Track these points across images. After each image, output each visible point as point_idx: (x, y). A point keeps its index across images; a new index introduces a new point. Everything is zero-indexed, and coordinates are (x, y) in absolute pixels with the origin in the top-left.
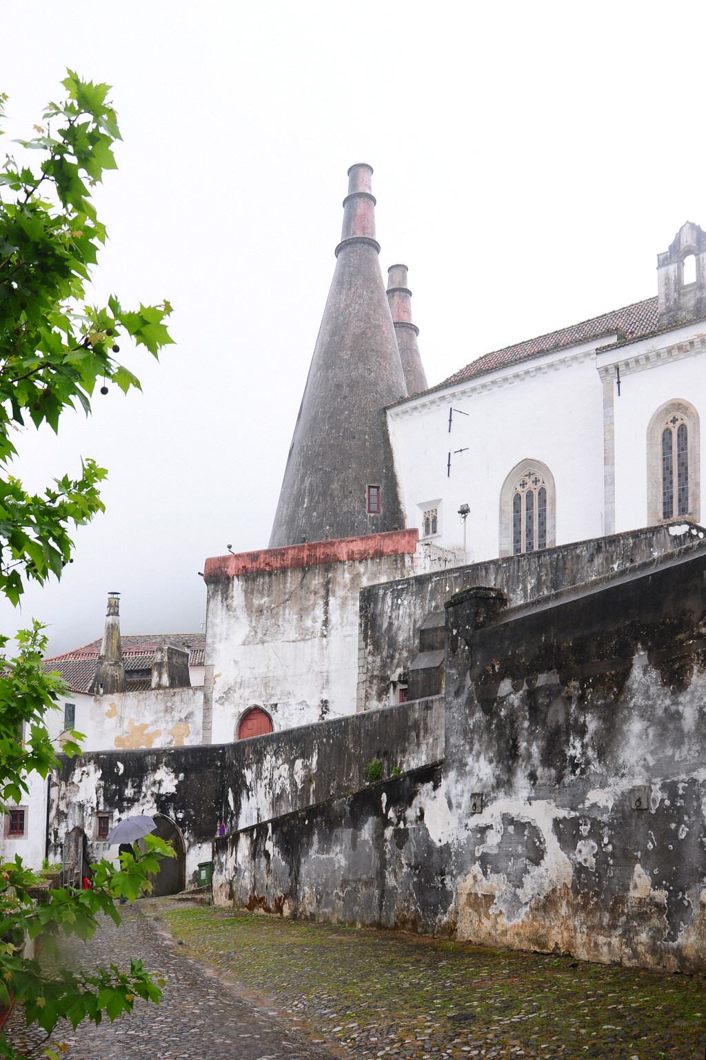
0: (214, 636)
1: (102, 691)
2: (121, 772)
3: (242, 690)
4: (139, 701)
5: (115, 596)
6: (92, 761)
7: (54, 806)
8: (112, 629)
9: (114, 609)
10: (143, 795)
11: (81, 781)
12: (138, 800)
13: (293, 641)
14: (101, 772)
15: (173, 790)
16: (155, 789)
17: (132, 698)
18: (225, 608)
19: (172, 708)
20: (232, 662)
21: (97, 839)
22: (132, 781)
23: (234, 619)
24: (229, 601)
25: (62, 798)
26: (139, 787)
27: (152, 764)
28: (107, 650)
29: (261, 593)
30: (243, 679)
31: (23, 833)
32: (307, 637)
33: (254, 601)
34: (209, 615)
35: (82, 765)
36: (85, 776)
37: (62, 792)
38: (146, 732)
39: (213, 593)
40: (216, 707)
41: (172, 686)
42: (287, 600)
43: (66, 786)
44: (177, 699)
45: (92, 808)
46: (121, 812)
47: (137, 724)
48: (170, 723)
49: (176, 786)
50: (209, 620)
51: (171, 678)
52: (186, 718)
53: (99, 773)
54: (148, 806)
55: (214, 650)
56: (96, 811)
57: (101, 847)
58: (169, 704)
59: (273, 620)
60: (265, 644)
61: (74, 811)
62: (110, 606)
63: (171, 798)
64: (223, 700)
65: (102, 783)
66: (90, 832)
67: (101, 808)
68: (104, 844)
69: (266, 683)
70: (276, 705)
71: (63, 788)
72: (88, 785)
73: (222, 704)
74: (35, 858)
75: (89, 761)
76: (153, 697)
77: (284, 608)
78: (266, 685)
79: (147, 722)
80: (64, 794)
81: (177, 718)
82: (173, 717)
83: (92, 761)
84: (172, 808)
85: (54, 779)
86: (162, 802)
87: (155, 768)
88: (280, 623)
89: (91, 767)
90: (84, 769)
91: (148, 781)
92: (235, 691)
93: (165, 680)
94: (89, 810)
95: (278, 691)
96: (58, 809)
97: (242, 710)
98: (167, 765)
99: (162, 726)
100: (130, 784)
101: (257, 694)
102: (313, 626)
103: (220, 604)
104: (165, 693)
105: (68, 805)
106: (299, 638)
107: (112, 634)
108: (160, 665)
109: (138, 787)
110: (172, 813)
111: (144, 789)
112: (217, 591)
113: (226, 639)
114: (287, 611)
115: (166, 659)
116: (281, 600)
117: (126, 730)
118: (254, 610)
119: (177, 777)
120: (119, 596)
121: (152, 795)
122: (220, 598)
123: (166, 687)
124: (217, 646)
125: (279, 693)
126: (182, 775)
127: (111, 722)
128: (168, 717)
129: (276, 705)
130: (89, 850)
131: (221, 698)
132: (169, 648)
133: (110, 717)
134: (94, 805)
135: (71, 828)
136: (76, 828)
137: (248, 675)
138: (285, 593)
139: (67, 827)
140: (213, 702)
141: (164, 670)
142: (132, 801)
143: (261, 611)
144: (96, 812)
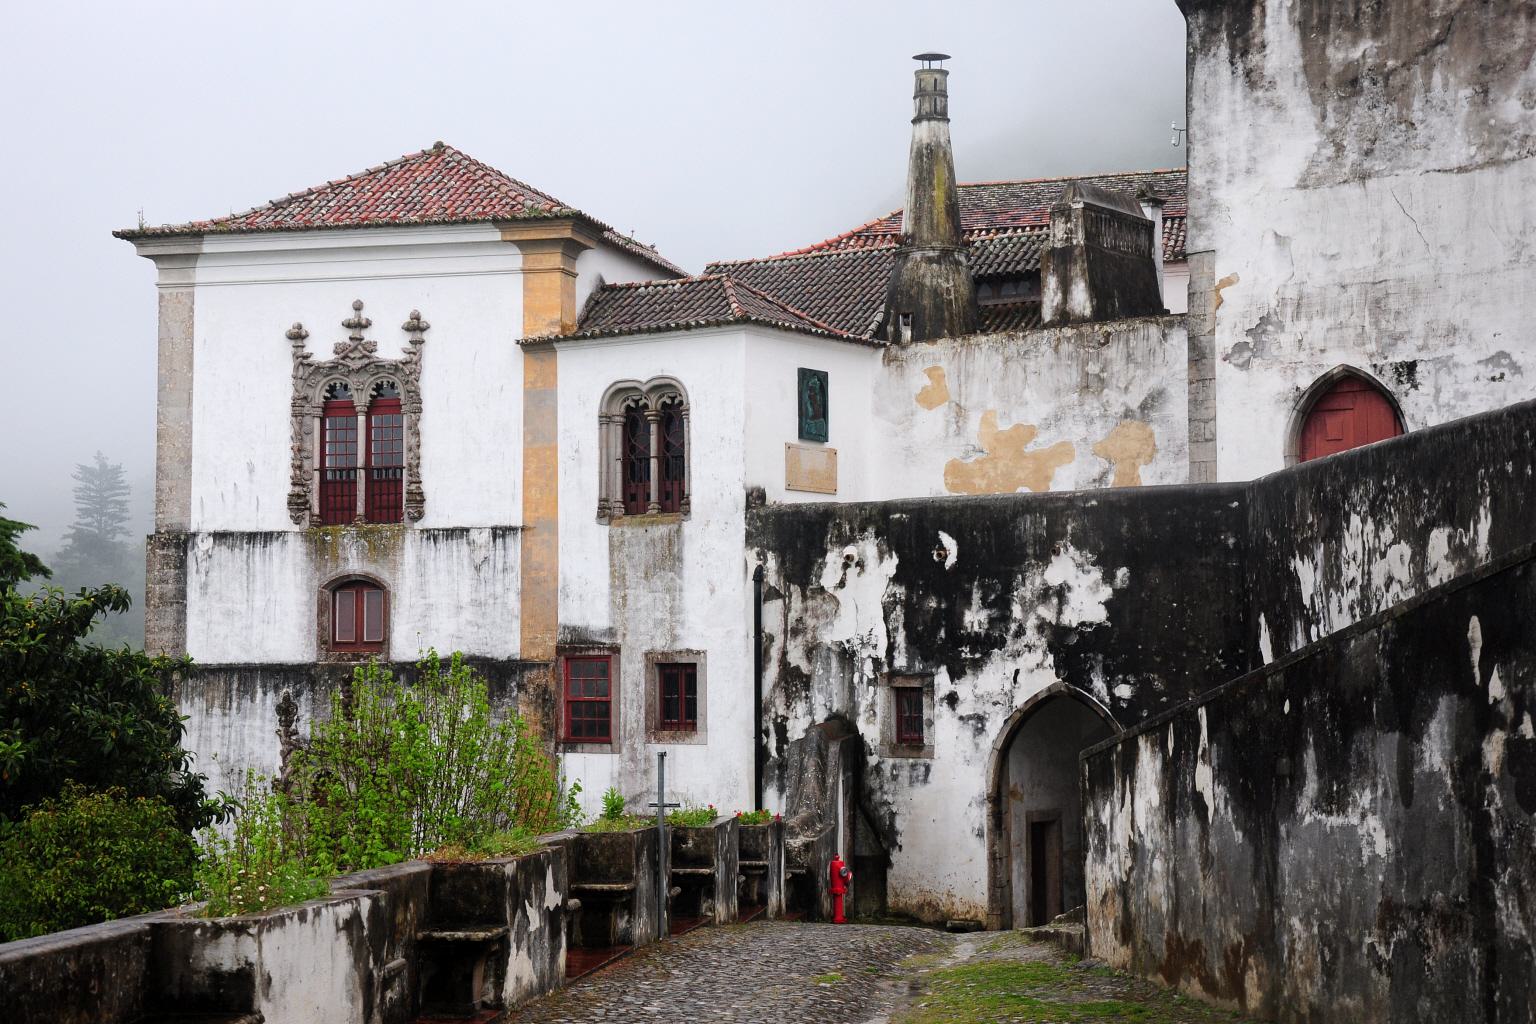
0: (1213, 165)
1: (907, 334)
2: (951, 560)
3: (1303, 324)
4: (1006, 361)
5: (936, 65)
6: (871, 530)
7: (775, 653)
8: (930, 162)
9: (932, 101)
10: (1013, 627)
11: (842, 584)
12: (1001, 643)
13: (1461, 170)
14: (895, 560)
15: (1099, 615)
16: (1047, 613)
17: (987, 354)
18: (1241, 81)
19: (1102, 380)
20: (1270, 240)
21: (894, 751)
22: (981, 586)
23: (1270, 112)
24: (1254, 59)
25: (795, 632)
27: (1038, 539)
28: (917, 220)
29: (1354, 28)
30: (1307, 289)
31: (693, 727)
32: (1508, 154)
33: (1330, 51)
34: (1196, 103)
35: (844, 541)
36: (853, 571)
37: (793, 616)
38: (1030, 448)
39: (1203, 40)
40: (1225, 373)
41: (1101, 314)
42: (1439, 42)
43: (804, 598)
44: (1114, 352)
45: (876, 662)
46: (956, 674)
47: (1004, 426)
48: (1099, 424)
49: (1108, 604)
50: (1195, 117)
51: (1095, 290)
52: (1143, 407)
53: (891, 564)
54: (1029, 660)
55: (1213, 205)
56: (886, 669)
57: (905, 773)
58: (1093, 368)
59: (1393, 109)
60: (1371, 183)
61: (827, 670)
62: (920, 93)
64: (1247, 352)
65: (900, 591)
66: (871, 731)
67: (900, 661)
68: (913, 767)
69: (1377, 301)
70: (1411, 367)
71: (796, 603)
72: (862, 597)
73: (1245, 366)
75: (863, 530)
76: (1044, 348)
77: (1429, 69)
78: (1377, 306)
79: (1034, 420)
80: (800, 620)
81: (1117, 409)
82: (1105, 406)
83: (871, 530)
84: (1099, 668)
85: (772, 579)
86: (1071, 649)
87: (1046, 553)
88: (1416, 115)
89: (868, 547)
90: (850, 550)
91: (1027, 590)
92: (1281, 327)
93: (1081, 300)
94: (868, 667)
95: (1417, 323)
97: (1306, 382)
98: (1079, 544)
99: (1075, 431)
100: (976, 596)
101: (1350, 333)
102: (1525, 120)
103: (1225, 70)
104: (1081, 336)
105: (811, 651)
106: (1479, 159)
107: (931, 172)
108: (1063, 257)
109: (1000, 606)
110: (1099, 684)
111: (1017, 611)
112: (1216, 31)
113: (1248, 171)
114: (1437, 78)
115: (1079, 239)
116: (1418, 42)
117: (975, 441)
118: (1330, 79)
119: (1108, 578)
120: (945, 65)
122: (1224, 51)
123: (1082, 320)
124: (1222, 194)
125: (1419, 329)
126: (1122, 573)
127: (932, 422)
128: (1092, 406)
129: (1411, 367)
130: (873, 782)
131: (1240, 347)
132: (1087, 207)
133: (930, 406)
134: (881, 653)
135: (820, 716)
136: (833, 717)
137: (1318, 276)
138: (1429, 22)
139: (810, 712)
140: (1218, 361)
141: (1077, 270)
142: (987, 644)
143: (1354, 82)
144: (886, 674)
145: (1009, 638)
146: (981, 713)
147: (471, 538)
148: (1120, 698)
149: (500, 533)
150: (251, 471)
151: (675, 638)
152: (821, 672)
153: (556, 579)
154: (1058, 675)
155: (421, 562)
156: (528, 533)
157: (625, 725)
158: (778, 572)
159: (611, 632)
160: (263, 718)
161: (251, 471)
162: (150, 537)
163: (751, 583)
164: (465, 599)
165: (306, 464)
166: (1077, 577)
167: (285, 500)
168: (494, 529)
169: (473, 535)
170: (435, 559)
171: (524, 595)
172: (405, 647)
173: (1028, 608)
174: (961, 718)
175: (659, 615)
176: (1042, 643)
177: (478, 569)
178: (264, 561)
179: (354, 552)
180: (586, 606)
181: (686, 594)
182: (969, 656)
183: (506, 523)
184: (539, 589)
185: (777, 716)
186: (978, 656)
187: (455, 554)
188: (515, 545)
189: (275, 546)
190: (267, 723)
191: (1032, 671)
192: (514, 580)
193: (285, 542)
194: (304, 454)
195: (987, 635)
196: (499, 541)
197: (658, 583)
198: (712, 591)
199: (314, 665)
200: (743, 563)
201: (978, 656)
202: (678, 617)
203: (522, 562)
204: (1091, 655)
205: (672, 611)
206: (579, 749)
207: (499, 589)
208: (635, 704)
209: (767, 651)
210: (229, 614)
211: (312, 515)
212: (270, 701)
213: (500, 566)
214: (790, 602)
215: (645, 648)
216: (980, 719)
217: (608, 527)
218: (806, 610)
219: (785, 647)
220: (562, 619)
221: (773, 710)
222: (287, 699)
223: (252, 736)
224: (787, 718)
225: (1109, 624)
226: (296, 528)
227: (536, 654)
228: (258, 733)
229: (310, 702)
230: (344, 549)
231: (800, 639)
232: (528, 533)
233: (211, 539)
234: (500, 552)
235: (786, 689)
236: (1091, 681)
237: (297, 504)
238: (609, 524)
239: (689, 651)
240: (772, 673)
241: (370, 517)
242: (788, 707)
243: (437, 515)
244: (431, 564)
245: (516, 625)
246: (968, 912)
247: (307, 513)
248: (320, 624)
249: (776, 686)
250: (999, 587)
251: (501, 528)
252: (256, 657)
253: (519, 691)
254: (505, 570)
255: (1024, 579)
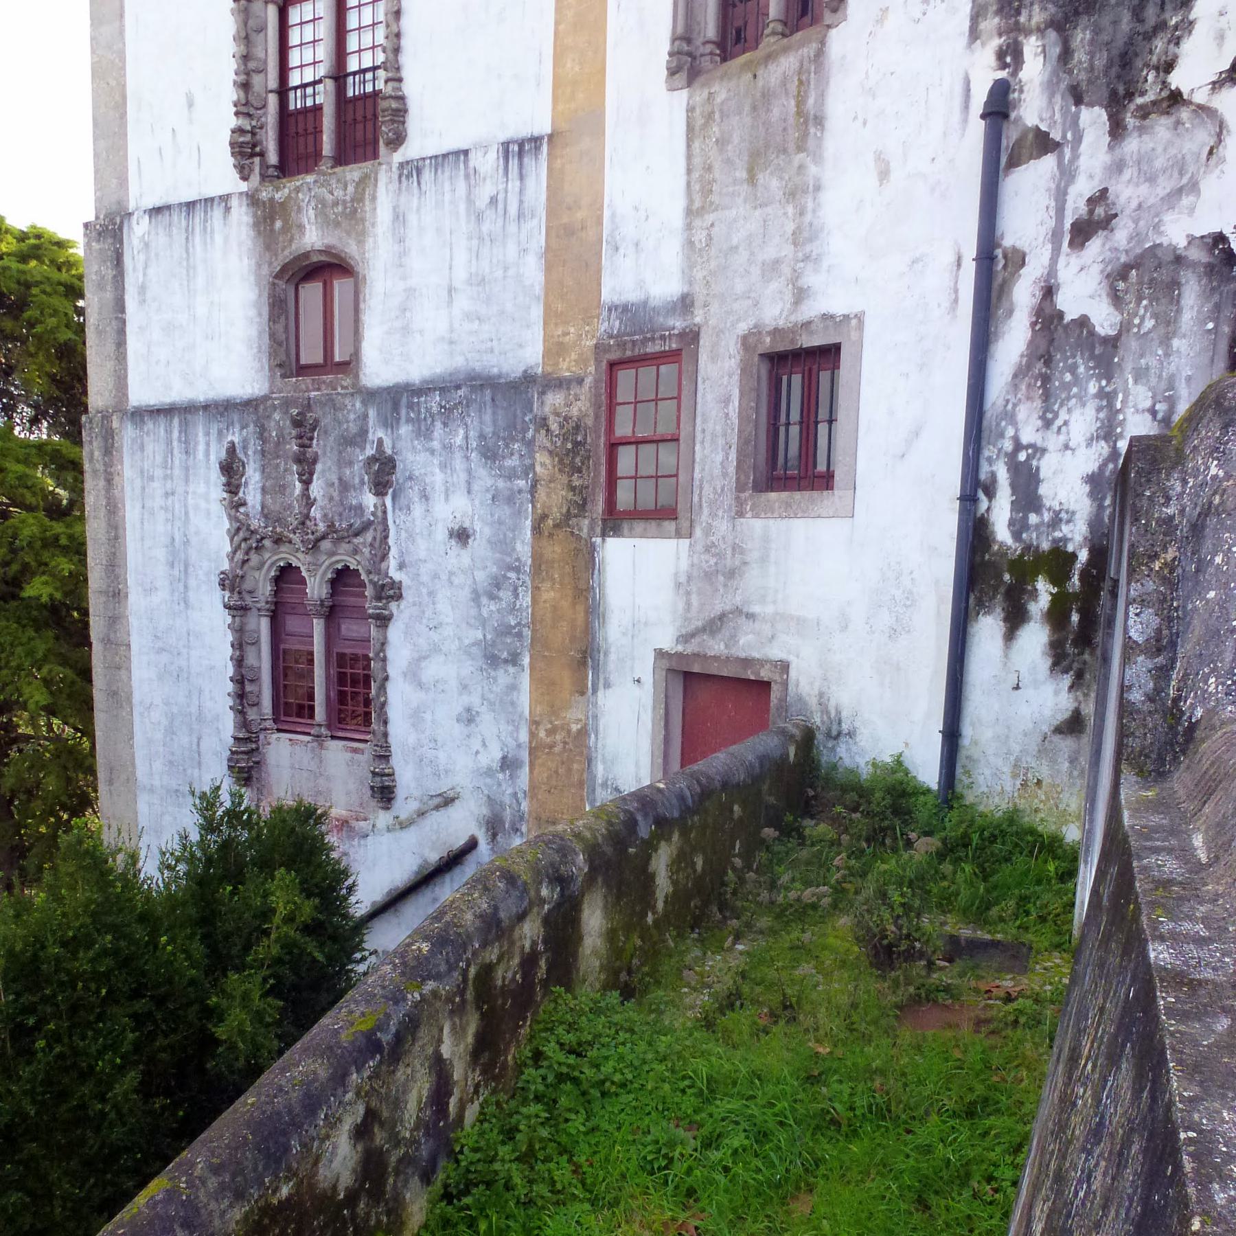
25: (1082, 232)
31: (826, 481)
43: (1117, 130)
74: (893, 633)
85: (1033, 109)
96: (1047, 318)
147: (471, 164)
149: (518, 150)
150: (191, 105)
151: (800, 295)
152: (1149, 324)
153: (599, 222)
155: (399, 218)
156: (557, 150)
157: (701, 488)
158: (1050, 87)
159: (685, 303)
160: (207, 482)
161: (191, 105)
162: (86, 225)
163: (977, 128)
164: (460, 275)
165: (257, 80)
167: (226, 137)
168: (506, 145)
169: (475, 159)
170: (418, 210)
171: (553, 259)
172: (380, 365)
175: (770, 253)
177: (479, 218)
178: (205, 243)
179: (311, 213)
180: (645, 267)
181: (826, 197)
183: (525, 132)
184: (574, 245)
185: (1018, 446)
187: (447, 197)
188: (538, 171)
189: (217, 212)
190: (212, 488)
192: (536, 233)
193: (228, 209)
194: (252, 65)
196: (514, 163)
197: (772, 183)
198: (884, 174)
199: (265, 398)
200: (959, 89)
202: (808, 248)
203: (548, 199)
205: (797, 239)
206: (626, 531)
207: (512, 250)
208: (721, 441)
209: (1005, 288)
210: (169, 328)
211: (264, 166)
212: (209, 450)
213: (513, 210)
214: (1075, 157)
215: (743, 327)
217: (684, 94)
218: (1118, 167)
219: (1052, 271)
220: (608, 294)
221: (1010, 432)
222: (232, 450)
223: (197, 508)
224: (1044, 451)
226: (244, 186)
227: (566, 368)
228: (203, 504)
229: (258, 457)
230: (299, 210)
231: (1095, 246)
232: (557, 150)
233: (147, 217)
234: (514, 185)
235: (1046, 379)
237: (245, 150)
238: (689, 84)
239: (827, 317)
240: (1014, 340)
241: (341, 159)
242: (1047, 424)
243: (421, 140)
244: (412, 219)
245: (537, 313)
247: (257, 160)
248: (272, 336)
249: (1020, 373)
251: (514, 142)
252: (200, 393)
253: (537, 431)
254: (520, 216)
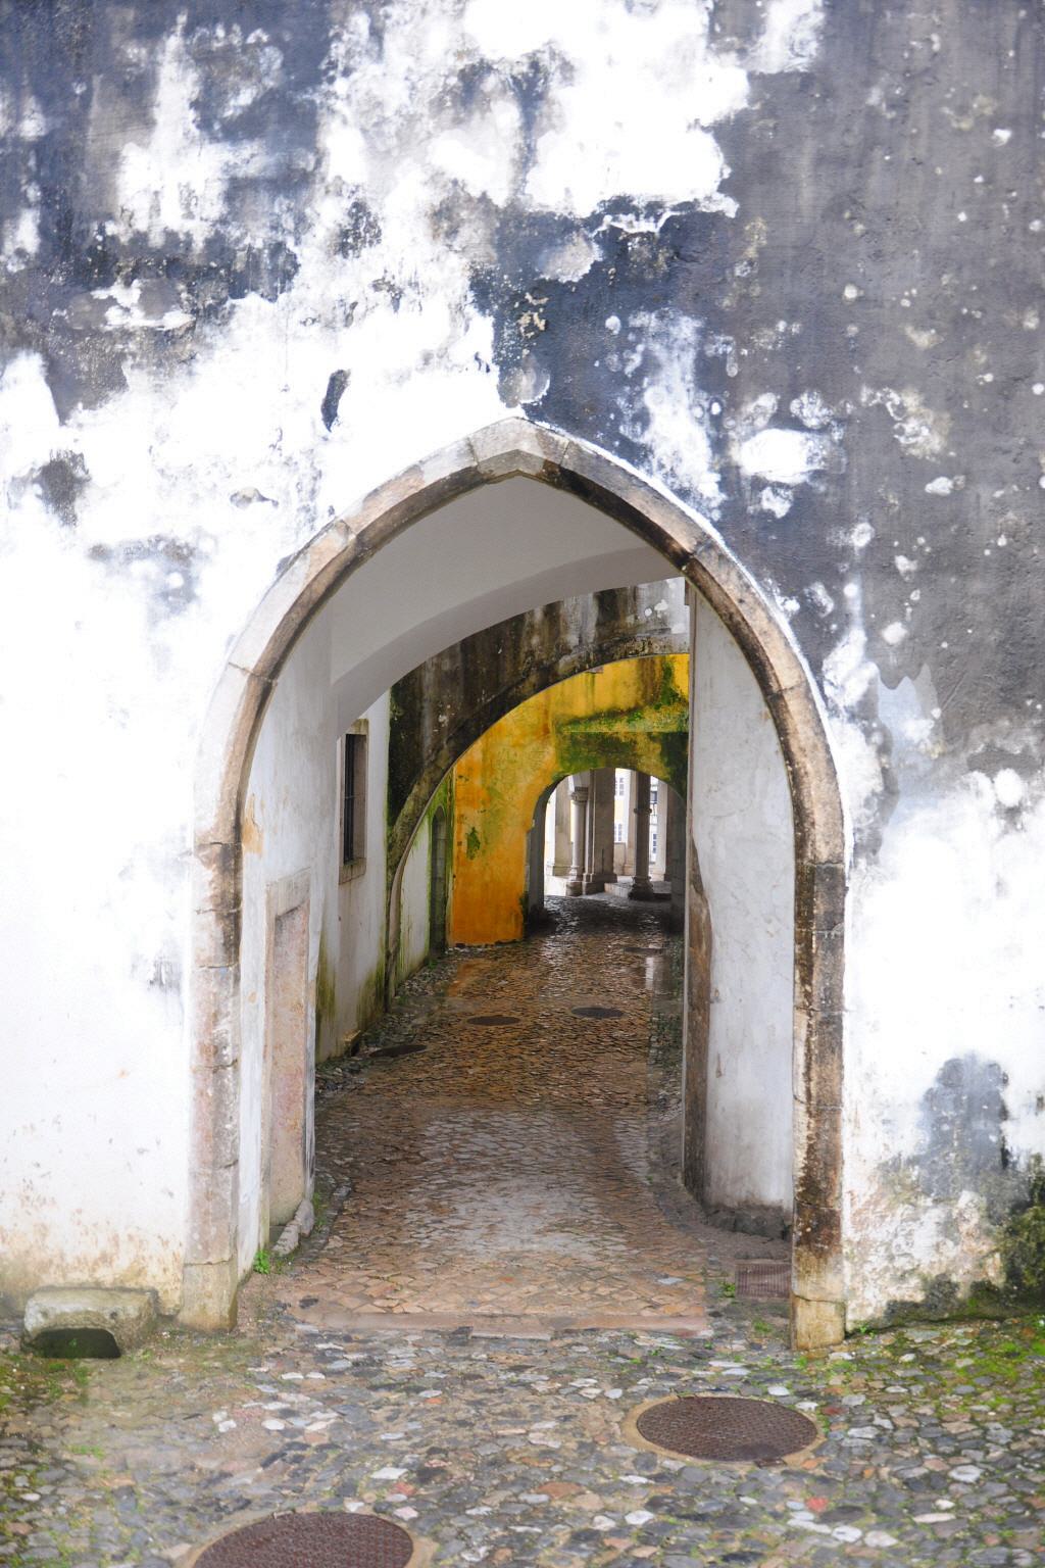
10: (329, 213)
12: (277, 271)
26: (290, 117)
49: (730, 134)
54: (376, 347)
63: (659, 262)
84: (678, 371)
86: (565, 302)
100: (175, 89)
111: (342, 149)
121: (444, 218)
142: (209, 277)
145: (310, 253)
146: (184, 536)
148: (758, 483)
154: (507, 394)
166: (603, 28)
173: (388, 137)
174: (99, 553)
176: (451, 274)
182: (138, 320)
186: (175, 319)
191: (402, 378)
195: (218, 245)
201: (175, 319)
204: (646, 320)
216: (180, 555)
225: (729, 207)
236: (643, 418)
246: (105, 1259)
250: (273, 58)
255: (377, 33)
